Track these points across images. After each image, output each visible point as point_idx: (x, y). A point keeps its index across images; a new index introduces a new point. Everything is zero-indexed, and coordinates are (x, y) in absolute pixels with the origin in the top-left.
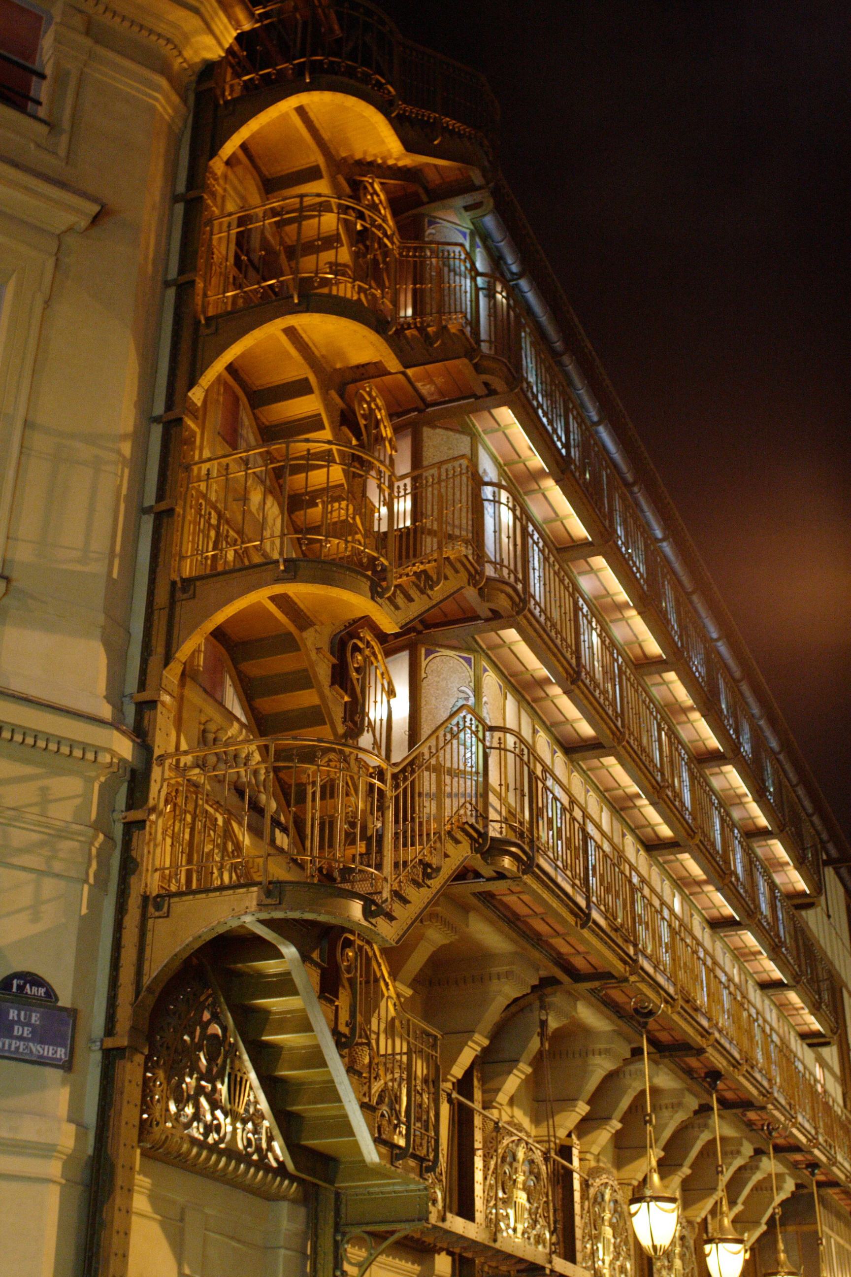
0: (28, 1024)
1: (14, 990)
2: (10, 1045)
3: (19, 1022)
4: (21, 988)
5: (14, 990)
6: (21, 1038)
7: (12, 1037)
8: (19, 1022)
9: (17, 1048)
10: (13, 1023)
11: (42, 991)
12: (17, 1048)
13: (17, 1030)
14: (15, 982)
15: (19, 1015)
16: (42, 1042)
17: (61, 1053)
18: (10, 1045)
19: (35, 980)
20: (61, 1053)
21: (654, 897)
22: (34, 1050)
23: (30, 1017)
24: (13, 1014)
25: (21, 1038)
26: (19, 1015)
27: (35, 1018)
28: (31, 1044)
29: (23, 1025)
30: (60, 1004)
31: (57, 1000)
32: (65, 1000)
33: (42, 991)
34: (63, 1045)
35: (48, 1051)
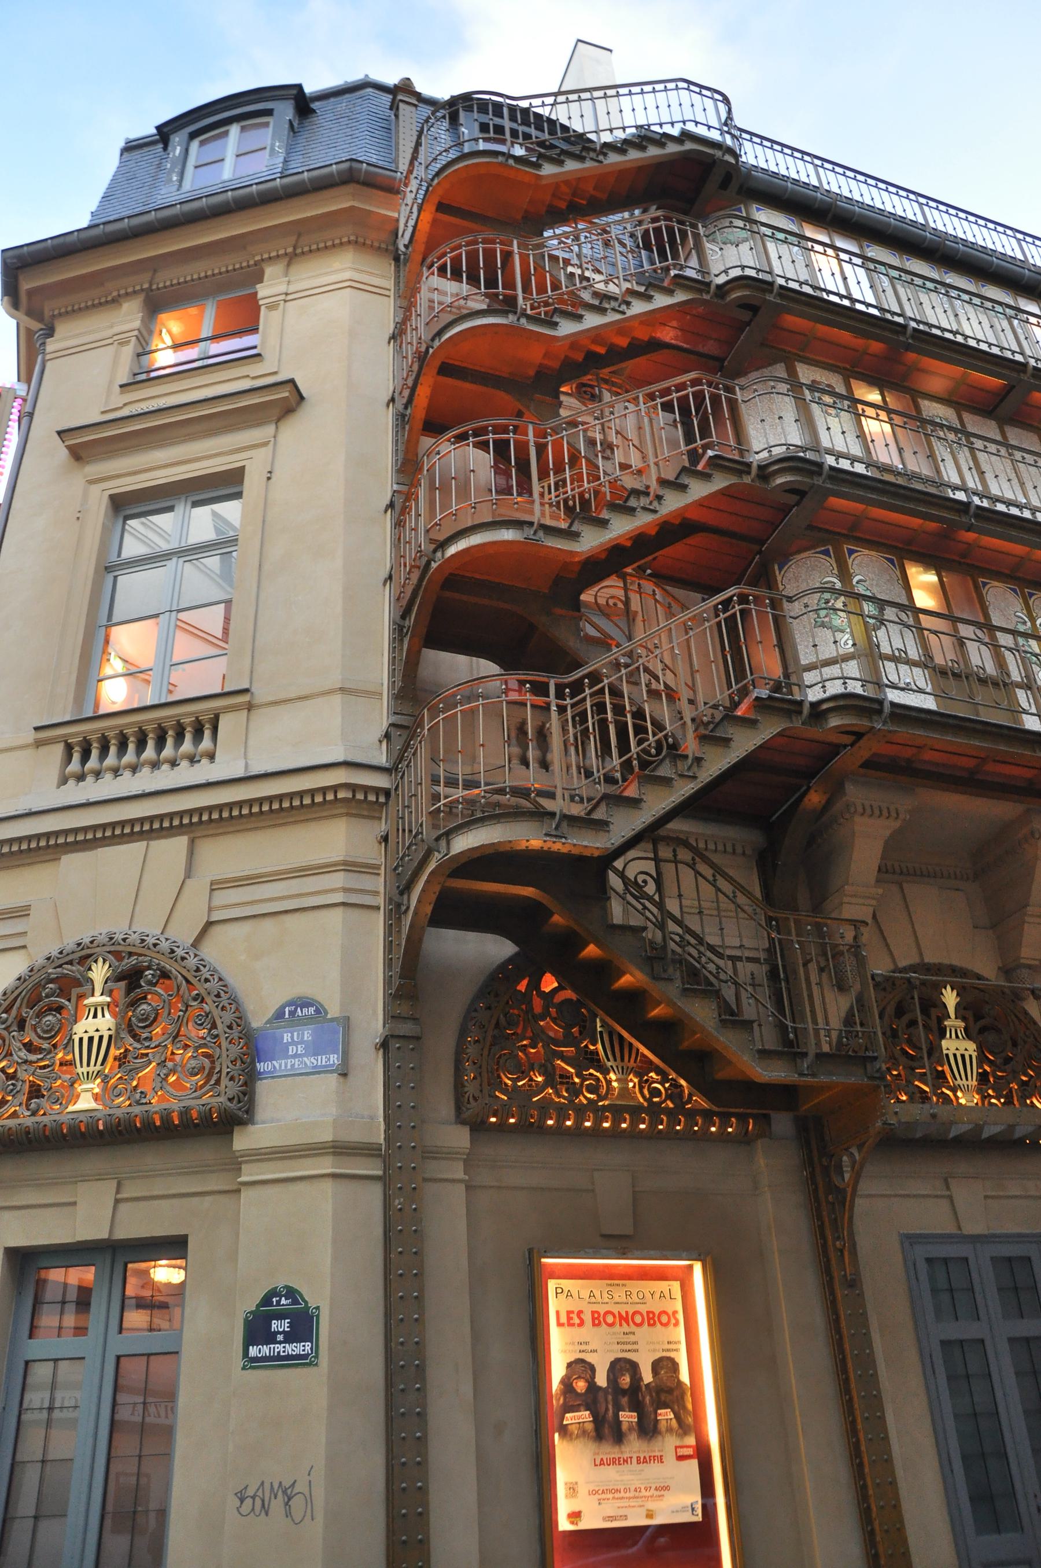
0: (302, 1042)
1: (287, 1016)
2: (286, 1065)
3: (293, 1043)
4: (292, 1013)
5: (287, 1016)
7: (287, 1057)
9: (293, 1065)
10: (289, 1044)
11: (312, 1010)
12: (293, 1065)
13: (292, 1050)
15: (292, 1037)
17: (334, 1059)
18: (286, 1065)
19: (305, 1003)
22: (308, 1063)
23: (303, 1034)
24: (287, 1037)
26: (292, 1037)
27: (307, 1036)
28: (305, 1059)
29: (296, 1044)
30: (329, 1016)
31: (326, 1013)
32: (334, 1011)
33: (312, 1010)
35: (322, 1060)
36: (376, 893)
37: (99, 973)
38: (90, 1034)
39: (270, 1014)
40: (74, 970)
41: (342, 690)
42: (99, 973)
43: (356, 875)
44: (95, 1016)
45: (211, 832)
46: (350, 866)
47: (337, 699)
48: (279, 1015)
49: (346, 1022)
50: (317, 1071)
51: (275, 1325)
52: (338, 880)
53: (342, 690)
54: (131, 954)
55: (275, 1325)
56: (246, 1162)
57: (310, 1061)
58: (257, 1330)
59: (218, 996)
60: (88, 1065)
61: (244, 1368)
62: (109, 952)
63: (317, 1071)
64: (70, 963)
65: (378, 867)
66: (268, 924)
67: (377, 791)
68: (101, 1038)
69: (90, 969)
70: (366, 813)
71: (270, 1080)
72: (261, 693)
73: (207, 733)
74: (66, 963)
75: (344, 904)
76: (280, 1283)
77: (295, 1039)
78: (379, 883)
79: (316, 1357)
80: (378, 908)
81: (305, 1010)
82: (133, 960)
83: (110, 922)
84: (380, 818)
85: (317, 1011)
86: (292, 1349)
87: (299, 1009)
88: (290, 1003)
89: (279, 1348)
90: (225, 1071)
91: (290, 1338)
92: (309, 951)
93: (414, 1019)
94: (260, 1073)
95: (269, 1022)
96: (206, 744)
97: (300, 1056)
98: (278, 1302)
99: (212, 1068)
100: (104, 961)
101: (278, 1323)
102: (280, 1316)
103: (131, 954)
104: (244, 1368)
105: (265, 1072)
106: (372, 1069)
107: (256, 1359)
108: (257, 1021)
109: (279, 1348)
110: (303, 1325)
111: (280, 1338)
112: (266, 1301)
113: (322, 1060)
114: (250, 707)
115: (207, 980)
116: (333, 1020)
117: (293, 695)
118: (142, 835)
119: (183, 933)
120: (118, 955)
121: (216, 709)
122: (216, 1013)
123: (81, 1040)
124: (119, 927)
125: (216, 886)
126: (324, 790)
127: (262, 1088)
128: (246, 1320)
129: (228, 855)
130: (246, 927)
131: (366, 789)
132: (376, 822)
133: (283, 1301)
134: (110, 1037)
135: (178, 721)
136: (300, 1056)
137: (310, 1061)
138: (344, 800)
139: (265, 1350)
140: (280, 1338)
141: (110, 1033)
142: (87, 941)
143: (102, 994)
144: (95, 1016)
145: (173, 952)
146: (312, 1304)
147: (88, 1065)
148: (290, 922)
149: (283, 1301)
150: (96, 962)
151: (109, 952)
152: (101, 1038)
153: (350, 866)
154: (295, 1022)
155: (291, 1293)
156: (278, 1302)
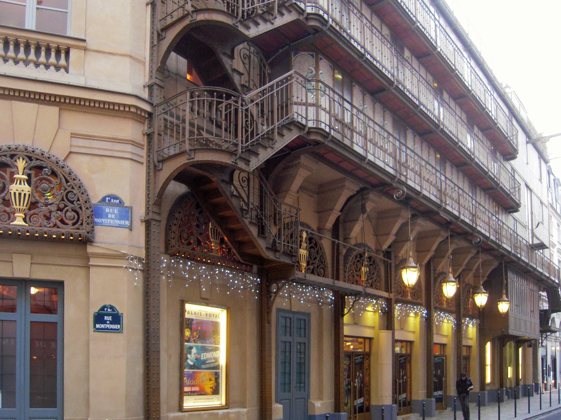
0: (114, 213)
4: (109, 201)
6: (111, 218)
8: (110, 213)
11: (118, 201)
13: (110, 216)
14: (107, 199)
16: (120, 219)
17: (127, 223)
19: (116, 198)
20: (127, 223)
21: (376, 126)
24: (107, 210)
25: (111, 218)
29: (111, 214)
31: (124, 204)
32: (127, 204)
33: (118, 201)
34: (128, 220)
35: (122, 222)
36: (142, 157)
37: (21, 164)
38: (24, 192)
39: (100, 198)
40: (7, 160)
41: (131, 57)
42: (21, 164)
43: (135, 147)
44: (20, 184)
45: (69, 108)
46: (134, 143)
47: (128, 60)
48: (104, 199)
49: (131, 208)
50: (120, 226)
51: (106, 318)
52: (129, 148)
53: (131, 57)
54: (37, 159)
55: (106, 318)
56: (93, 257)
57: (118, 222)
58: (99, 318)
59: (80, 187)
60: (20, 205)
61: (94, 331)
62: (26, 156)
63: (120, 226)
64: (5, 156)
65: (143, 146)
66: (97, 159)
67: (145, 111)
68: (25, 195)
69: (16, 161)
70: (139, 120)
71: (101, 227)
72: (91, 44)
73: (63, 56)
74: (4, 156)
75: (131, 159)
76: (108, 303)
77: (111, 212)
78: (144, 152)
79: (122, 330)
80: (142, 163)
81: (115, 201)
82: (38, 163)
83: (22, 140)
84: (144, 123)
85: (120, 202)
86: (113, 326)
87: (111, 199)
88: (109, 196)
89: (108, 326)
90: (85, 220)
91: (111, 323)
92: (117, 177)
93: (159, 214)
94: (96, 223)
95: (99, 202)
96: (63, 62)
97: (113, 219)
98: (107, 310)
99: (79, 218)
100: (23, 159)
101: (106, 318)
102: (108, 315)
103: (37, 159)
104: (94, 331)
105: (98, 223)
106: (140, 230)
107: (98, 329)
108: (94, 200)
109: (108, 326)
110: (117, 319)
111: (108, 322)
112: (103, 309)
113: (122, 222)
114: (85, 49)
115: (74, 180)
116: (126, 207)
117: (107, 51)
118: (34, 100)
119: (58, 152)
120: (30, 158)
121: (69, 44)
122: (80, 195)
123: (15, 193)
124: (28, 143)
125: (74, 135)
126: (124, 106)
127: (97, 228)
128: (94, 315)
129: (79, 122)
130: (88, 158)
131: (142, 110)
132: (142, 125)
133: (109, 310)
134: (29, 195)
135: (48, 44)
136: (113, 219)
137: (118, 222)
138: (132, 112)
139: (102, 326)
140: (108, 322)
141: (30, 193)
142: (13, 147)
143: (23, 174)
144: (20, 184)
145: (57, 163)
146: (120, 312)
147: (20, 205)
148: (107, 160)
149: (109, 310)
150: (19, 158)
151: (26, 156)
152: (25, 195)
153: (134, 143)
154: (110, 204)
155: (112, 308)
156: (107, 310)
